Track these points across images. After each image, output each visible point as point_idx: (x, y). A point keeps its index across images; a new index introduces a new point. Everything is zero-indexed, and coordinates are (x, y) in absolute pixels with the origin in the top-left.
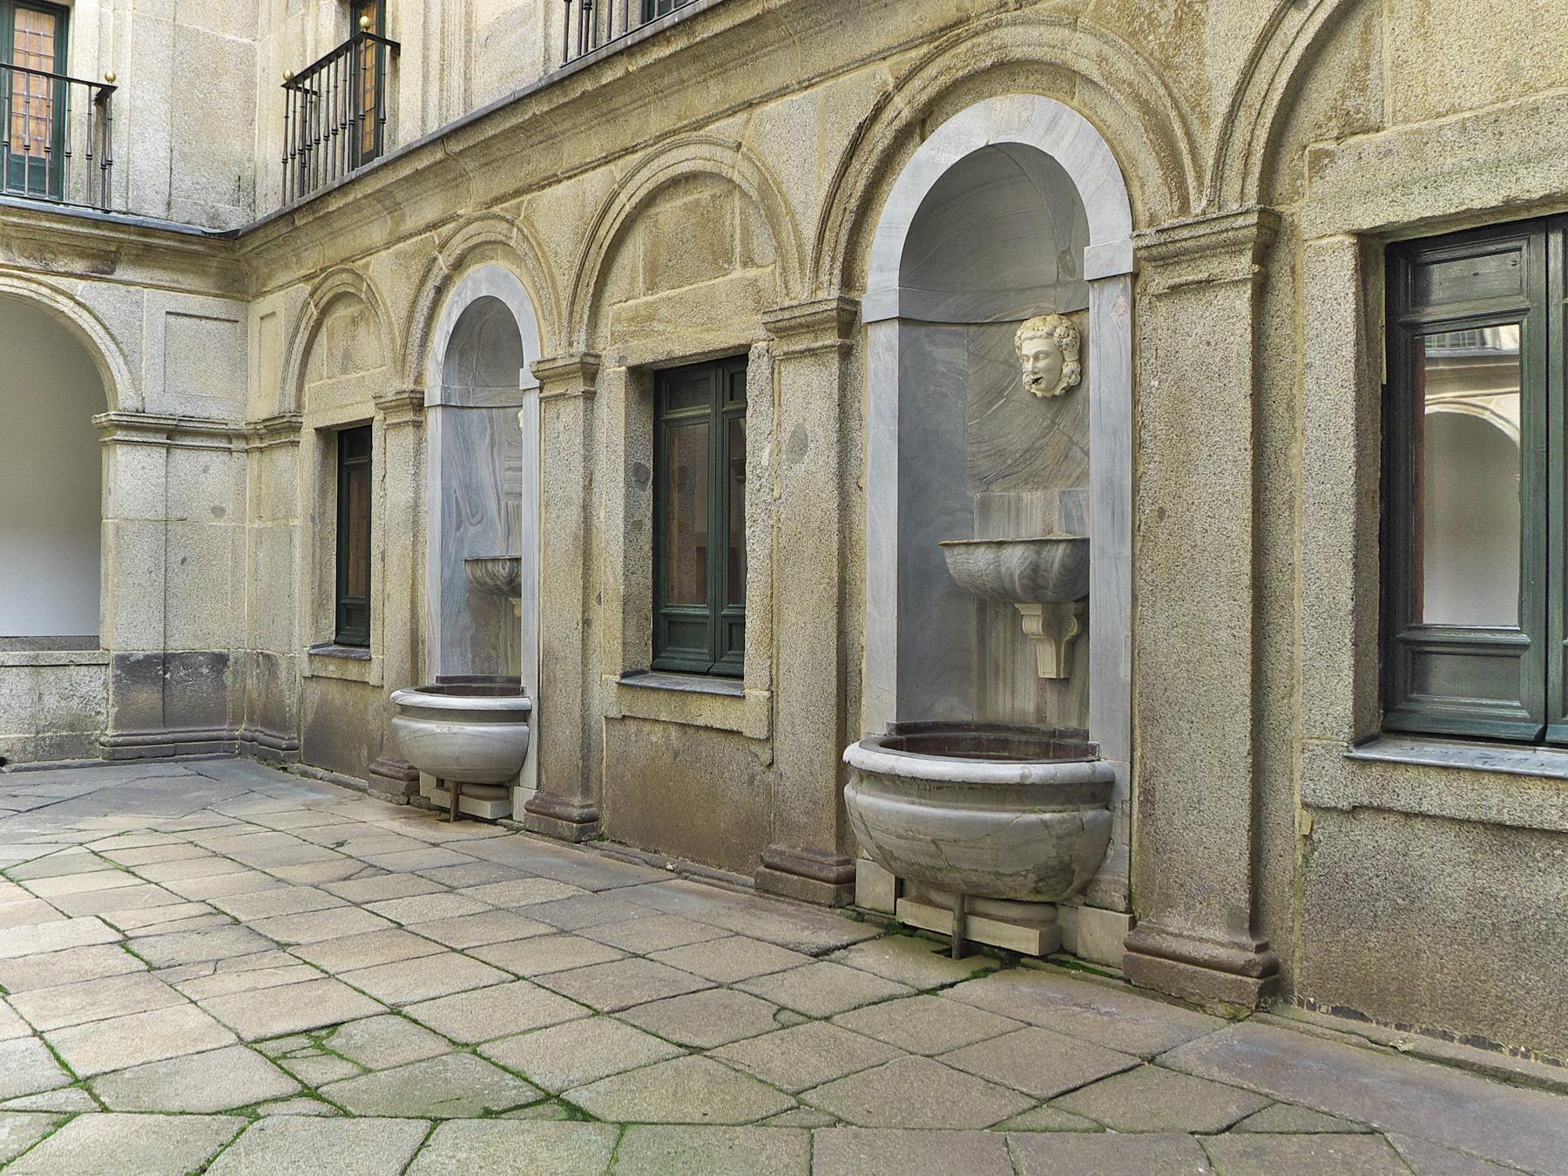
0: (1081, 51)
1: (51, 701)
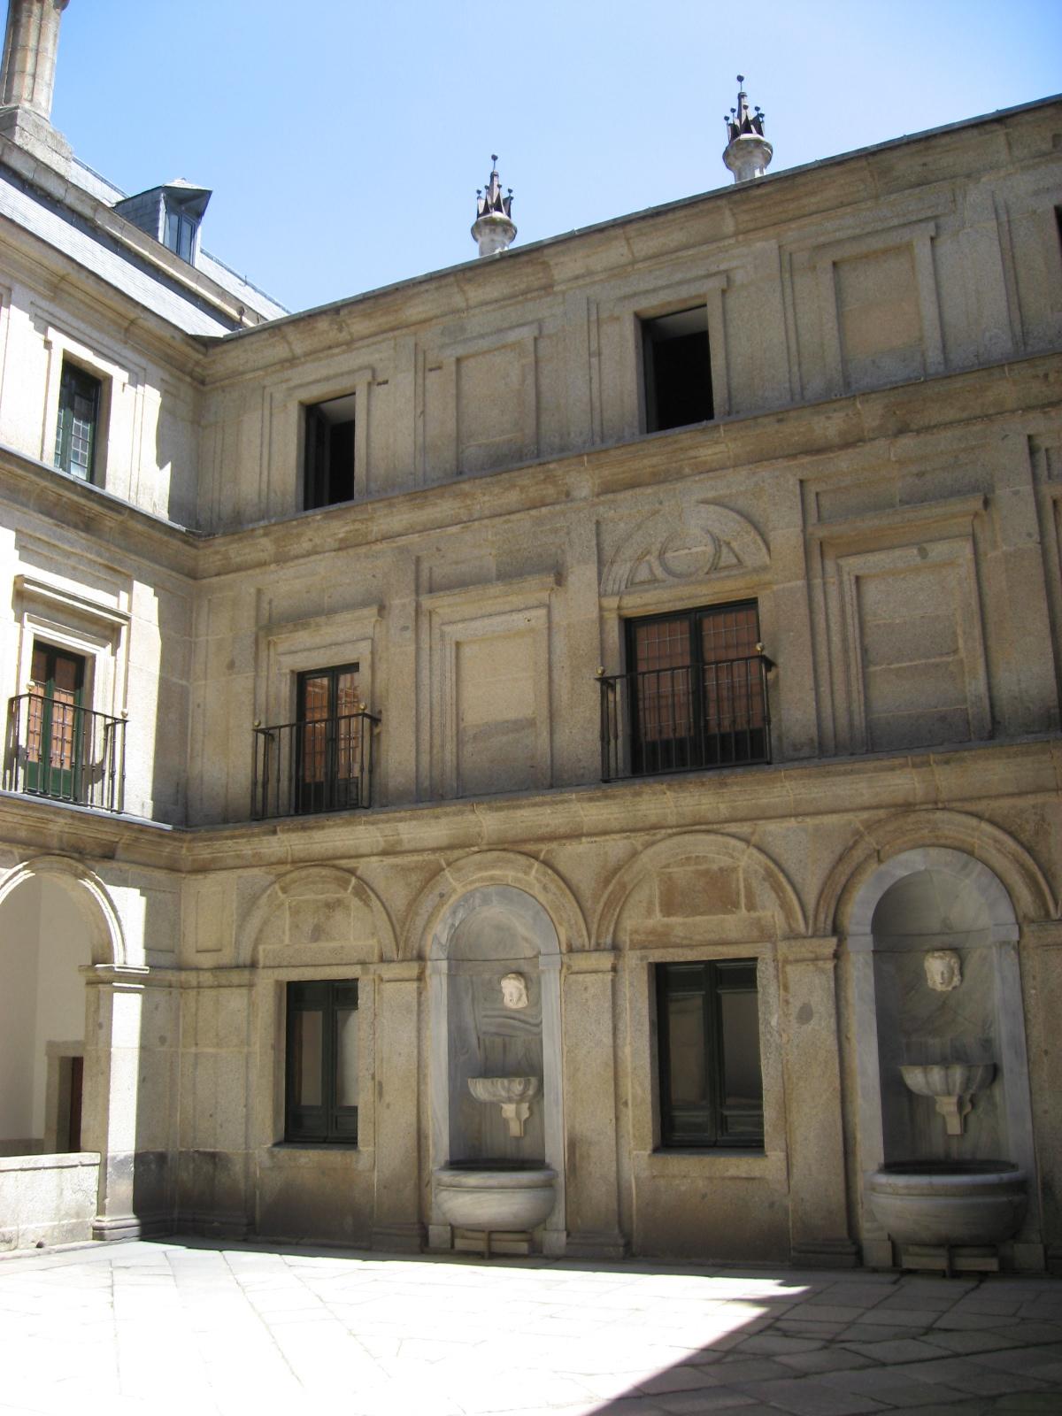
1: (67, 1193)
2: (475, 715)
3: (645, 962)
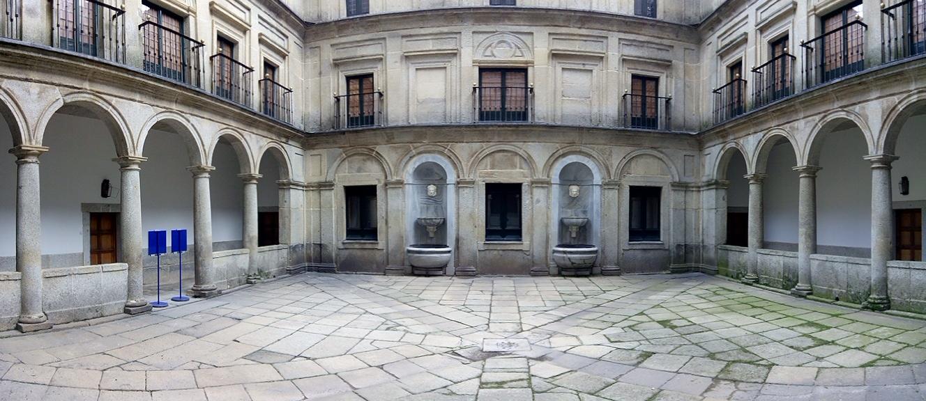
0: (594, 154)
2: (422, 97)
3: (484, 183)
